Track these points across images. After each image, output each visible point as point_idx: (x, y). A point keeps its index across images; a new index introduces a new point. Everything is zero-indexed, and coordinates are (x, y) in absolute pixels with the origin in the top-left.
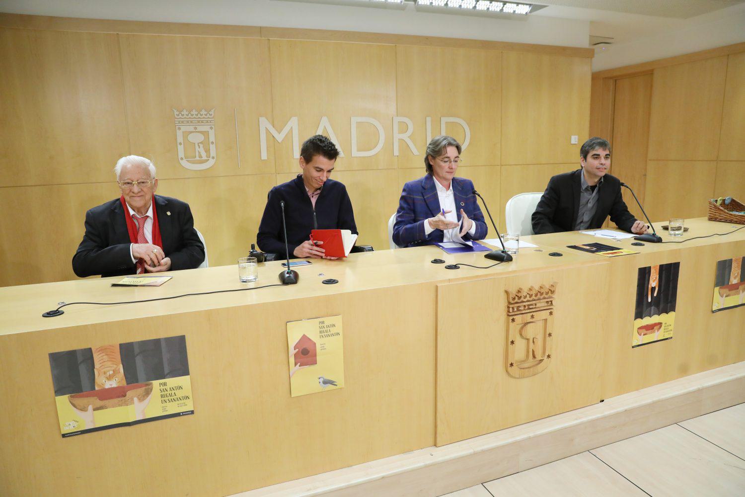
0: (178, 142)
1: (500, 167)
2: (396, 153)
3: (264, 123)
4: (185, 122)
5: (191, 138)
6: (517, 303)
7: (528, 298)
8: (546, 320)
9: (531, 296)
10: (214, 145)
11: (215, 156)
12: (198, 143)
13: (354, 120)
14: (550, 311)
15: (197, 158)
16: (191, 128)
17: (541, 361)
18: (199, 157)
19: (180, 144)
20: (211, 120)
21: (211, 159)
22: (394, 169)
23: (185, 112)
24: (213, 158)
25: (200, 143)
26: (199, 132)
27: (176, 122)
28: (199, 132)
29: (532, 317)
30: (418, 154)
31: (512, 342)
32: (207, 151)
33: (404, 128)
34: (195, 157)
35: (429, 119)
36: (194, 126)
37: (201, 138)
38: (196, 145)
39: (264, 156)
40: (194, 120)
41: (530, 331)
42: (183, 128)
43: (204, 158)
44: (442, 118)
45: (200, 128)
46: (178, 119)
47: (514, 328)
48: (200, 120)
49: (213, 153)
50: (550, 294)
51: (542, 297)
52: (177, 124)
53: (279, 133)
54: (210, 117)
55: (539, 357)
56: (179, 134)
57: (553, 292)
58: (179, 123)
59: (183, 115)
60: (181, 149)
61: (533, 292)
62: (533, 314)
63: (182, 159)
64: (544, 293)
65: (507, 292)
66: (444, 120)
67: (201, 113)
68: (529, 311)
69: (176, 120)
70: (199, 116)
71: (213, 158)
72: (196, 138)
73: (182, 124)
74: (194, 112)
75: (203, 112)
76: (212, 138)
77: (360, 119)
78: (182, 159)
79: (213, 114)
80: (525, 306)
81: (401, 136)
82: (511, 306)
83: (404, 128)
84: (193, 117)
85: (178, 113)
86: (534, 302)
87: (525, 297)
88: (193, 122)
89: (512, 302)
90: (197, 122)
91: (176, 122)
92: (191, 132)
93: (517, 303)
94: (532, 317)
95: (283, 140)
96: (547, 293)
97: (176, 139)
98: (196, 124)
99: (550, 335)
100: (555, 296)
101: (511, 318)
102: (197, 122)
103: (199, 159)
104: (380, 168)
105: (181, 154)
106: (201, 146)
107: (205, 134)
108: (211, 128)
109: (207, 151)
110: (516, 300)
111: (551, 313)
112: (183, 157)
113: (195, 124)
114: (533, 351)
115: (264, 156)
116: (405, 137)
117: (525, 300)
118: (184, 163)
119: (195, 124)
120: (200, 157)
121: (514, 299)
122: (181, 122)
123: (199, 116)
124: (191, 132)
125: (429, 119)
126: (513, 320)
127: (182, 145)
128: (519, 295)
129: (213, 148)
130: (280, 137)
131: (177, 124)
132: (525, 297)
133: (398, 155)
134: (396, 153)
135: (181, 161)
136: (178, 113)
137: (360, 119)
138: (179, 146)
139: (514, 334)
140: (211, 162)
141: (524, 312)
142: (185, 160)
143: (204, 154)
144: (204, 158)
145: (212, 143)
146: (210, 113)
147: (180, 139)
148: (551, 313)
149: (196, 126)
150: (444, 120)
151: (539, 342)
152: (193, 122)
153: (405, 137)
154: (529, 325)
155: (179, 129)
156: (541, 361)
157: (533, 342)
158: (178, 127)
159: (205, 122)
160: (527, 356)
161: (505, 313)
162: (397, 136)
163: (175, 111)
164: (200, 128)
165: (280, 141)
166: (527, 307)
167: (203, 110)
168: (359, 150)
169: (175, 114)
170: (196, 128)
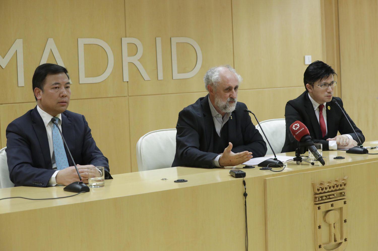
2: (126, 78)
6: (321, 193)
7: (328, 190)
8: (341, 209)
9: (330, 188)
13: (82, 42)
14: (344, 200)
17: (340, 243)
22: (125, 96)
29: (332, 205)
30: (150, 79)
31: (320, 227)
33: (133, 50)
41: (333, 217)
44: (172, 38)
47: (320, 213)
50: (343, 186)
53: (3, 58)
55: (339, 241)
57: (345, 185)
66: (175, 41)
80: (326, 196)
82: (317, 196)
86: (333, 193)
87: (326, 188)
89: (318, 192)
93: (321, 193)
94: (332, 205)
95: (6, 67)
96: (341, 186)
99: (345, 221)
100: (346, 187)
101: (318, 206)
104: (109, 96)
110: (320, 191)
111: (345, 203)
114: (335, 235)
116: (135, 59)
117: (326, 191)
121: (318, 190)
125: (159, 40)
126: (319, 208)
128: (322, 186)
132: (326, 188)
133: (128, 81)
139: (320, 221)
148: (345, 203)
151: (338, 226)
153: (135, 59)
154: (330, 212)
156: (340, 243)
157: (334, 227)
160: (330, 241)
161: (313, 203)
162: (126, 59)
166: (328, 197)
168: (87, 76)
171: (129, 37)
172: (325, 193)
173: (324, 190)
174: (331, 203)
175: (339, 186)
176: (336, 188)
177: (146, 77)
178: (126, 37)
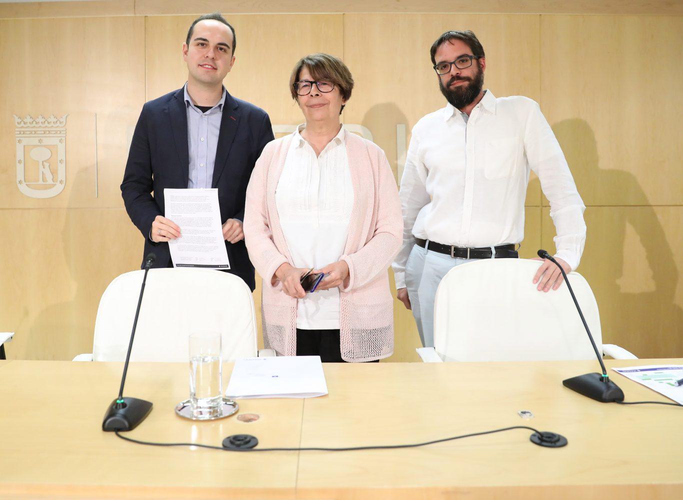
0: (18, 159)
4: (28, 133)
5: (35, 154)
10: (64, 165)
11: (64, 179)
12: (43, 162)
15: (41, 182)
16: (35, 141)
18: (43, 181)
19: (20, 162)
20: (61, 129)
21: (58, 184)
24: (61, 182)
25: (45, 161)
26: (45, 146)
28: (45, 146)
32: (54, 173)
34: (38, 181)
36: (39, 139)
37: (47, 154)
42: (25, 141)
43: (50, 182)
48: (47, 129)
49: (61, 175)
54: (60, 125)
58: (20, 133)
59: (25, 123)
60: (20, 168)
63: (20, 182)
67: (49, 120)
69: (17, 130)
71: (61, 182)
74: (40, 120)
75: (52, 119)
76: (62, 156)
78: (20, 182)
79: (65, 122)
84: (38, 125)
85: (19, 120)
88: (38, 132)
92: (35, 146)
97: (15, 156)
98: (44, 135)
102: (41, 132)
103: (43, 183)
105: (20, 176)
106: (47, 165)
107: (52, 148)
109: (54, 173)
112: (23, 180)
118: (23, 188)
122: (22, 133)
124: (35, 146)
127: (22, 164)
129: (61, 169)
131: (16, 136)
135: (19, 186)
136: (19, 120)
138: (18, 164)
140: (59, 188)
142: (24, 184)
145: (61, 161)
146: (61, 120)
147: (20, 155)
149: (42, 138)
152: (38, 132)
155: (20, 141)
158: (18, 139)
159: (54, 132)
163: (16, 118)
164: (47, 141)
167: (52, 117)
169: (16, 122)
170: (40, 141)
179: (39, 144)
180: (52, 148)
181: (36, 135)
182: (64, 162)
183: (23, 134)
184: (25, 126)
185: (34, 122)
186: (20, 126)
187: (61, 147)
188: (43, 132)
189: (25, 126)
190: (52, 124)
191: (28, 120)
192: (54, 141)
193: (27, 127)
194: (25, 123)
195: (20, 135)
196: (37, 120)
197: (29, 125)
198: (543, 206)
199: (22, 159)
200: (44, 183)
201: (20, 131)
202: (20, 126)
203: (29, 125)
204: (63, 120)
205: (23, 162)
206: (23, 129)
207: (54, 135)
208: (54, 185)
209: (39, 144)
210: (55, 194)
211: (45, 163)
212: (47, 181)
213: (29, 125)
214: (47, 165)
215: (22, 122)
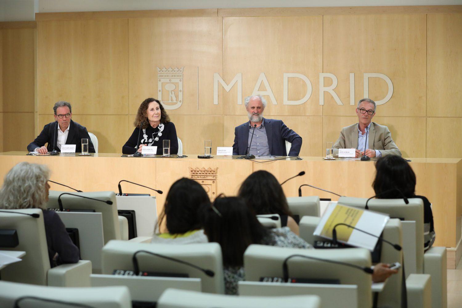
0: (159, 89)
1: (425, 118)
3: (218, 78)
7: (200, 172)
10: (182, 92)
13: (286, 76)
14: (213, 181)
15: (170, 101)
16: (168, 80)
19: (160, 91)
20: (181, 74)
23: (164, 69)
24: (180, 101)
25: (173, 91)
26: (173, 83)
27: (158, 76)
28: (173, 83)
32: (177, 97)
33: (328, 82)
34: (169, 101)
35: (352, 76)
37: (173, 87)
38: (170, 92)
39: (216, 102)
40: (168, 74)
42: (163, 80)
43: (175, 101)
45: (173, 81)
46: (160, 74)
49: (180, 98)
51: (208, 173)
52: (158, 78)
56: (160, 84)
58: (160, 76)
59: (162, 71)
61: (203, 170)
62: (204, 181)
64: (209, 171)
65: (189, 168)
66: (366, 76)
67: (175, 70)
68: (200, 179)
70: (173, 72)
72: (169, 87)
73: (162, 77)
74: (170, 69)
75: (176, 69)
76: (181, 88)
77: (291, 75)
79: (182, 71)
81: (327, 89)
83: (328, 82)
88: (169, 76)
90: (171, 76)
91: (158, 76)
103: (171, 102)
104: (307, 115)
106: (173, 92)
107: (176, 84)
108: (180, 81)
109: (177, 97)
113: (170, 78)
115: (216, 102)
116: (330, 89)
117: (198, 173)
119: (170, 78)
120: (172, 100)
122: (161, 76)
123: (173, 72)
127: (161, 92)
129: (180, 95)
130: (227, 88)
131: (158, 78)
134: (321, 103)
137: (291, 75)
138: (158, 92)
140: (179, 104)
141: (198, 179)
143: (174, 99)
144: (175, 101)
145: (180, 91)
146: (181, 70)
147: (160, 88)
148: (214, 182)
150: (366, 76)
152: (169, 76)
153: (330, 89)
155: (160, 80)
158: (159, 79)
162: (322, 89)
164: (173, 81)
165: (228, 90)
170: (170, 80)
171: (326, 72)
172: (197, 173)
173: (197, 172)
174: (202, 180)
175: (209, 171)
176: (206, 172)
177: (339, 102)
178: (323, 73)
179: (170, 82)
180: (176, 84)
181: (168, 77)
182: (182, 91)
183: (162, 76)
184: (163, 73)
185: (167, 71)
186: (160, 73)
187: (180, 84)
188: (171, 76)
189: (163, 73)
190: (176, 72)
191: (164, 69)
192: (176, 80)
193: (163, 73)
194: (162, 71)
195: (161, 77)
196: (169, 70)
197: (165, 72)
198: (428, 117)
199: (161, 90)
200: (171, 102)
201: (160, 75)
202: (160, 73)
203: (165, 72)
204: (182, 70)
205: (161, 91)
206: (161, 74)
207: (177, 78)
208: (177, 103)
209: (170, 82)
210: (177, 108)
211: (172, 92)
212: (173, 101)
213: (164, 72)
214: (173, 92)
215: (161, 71)
